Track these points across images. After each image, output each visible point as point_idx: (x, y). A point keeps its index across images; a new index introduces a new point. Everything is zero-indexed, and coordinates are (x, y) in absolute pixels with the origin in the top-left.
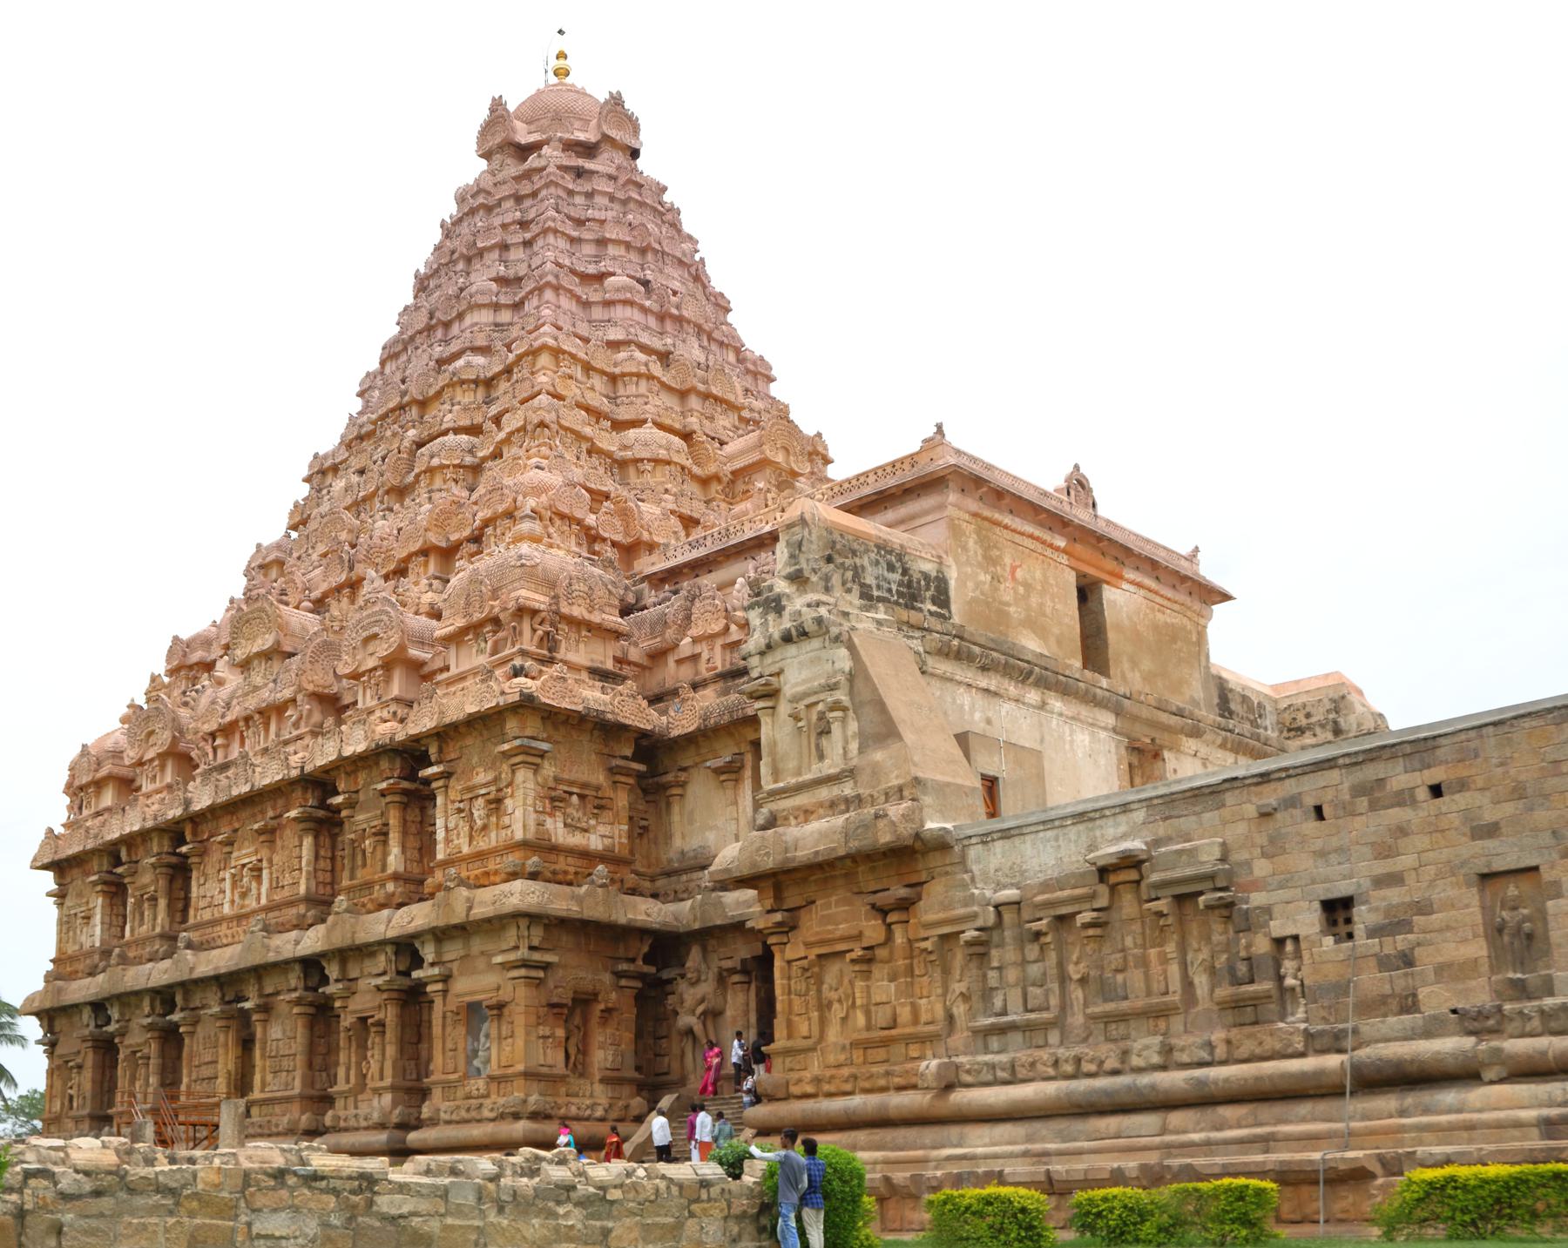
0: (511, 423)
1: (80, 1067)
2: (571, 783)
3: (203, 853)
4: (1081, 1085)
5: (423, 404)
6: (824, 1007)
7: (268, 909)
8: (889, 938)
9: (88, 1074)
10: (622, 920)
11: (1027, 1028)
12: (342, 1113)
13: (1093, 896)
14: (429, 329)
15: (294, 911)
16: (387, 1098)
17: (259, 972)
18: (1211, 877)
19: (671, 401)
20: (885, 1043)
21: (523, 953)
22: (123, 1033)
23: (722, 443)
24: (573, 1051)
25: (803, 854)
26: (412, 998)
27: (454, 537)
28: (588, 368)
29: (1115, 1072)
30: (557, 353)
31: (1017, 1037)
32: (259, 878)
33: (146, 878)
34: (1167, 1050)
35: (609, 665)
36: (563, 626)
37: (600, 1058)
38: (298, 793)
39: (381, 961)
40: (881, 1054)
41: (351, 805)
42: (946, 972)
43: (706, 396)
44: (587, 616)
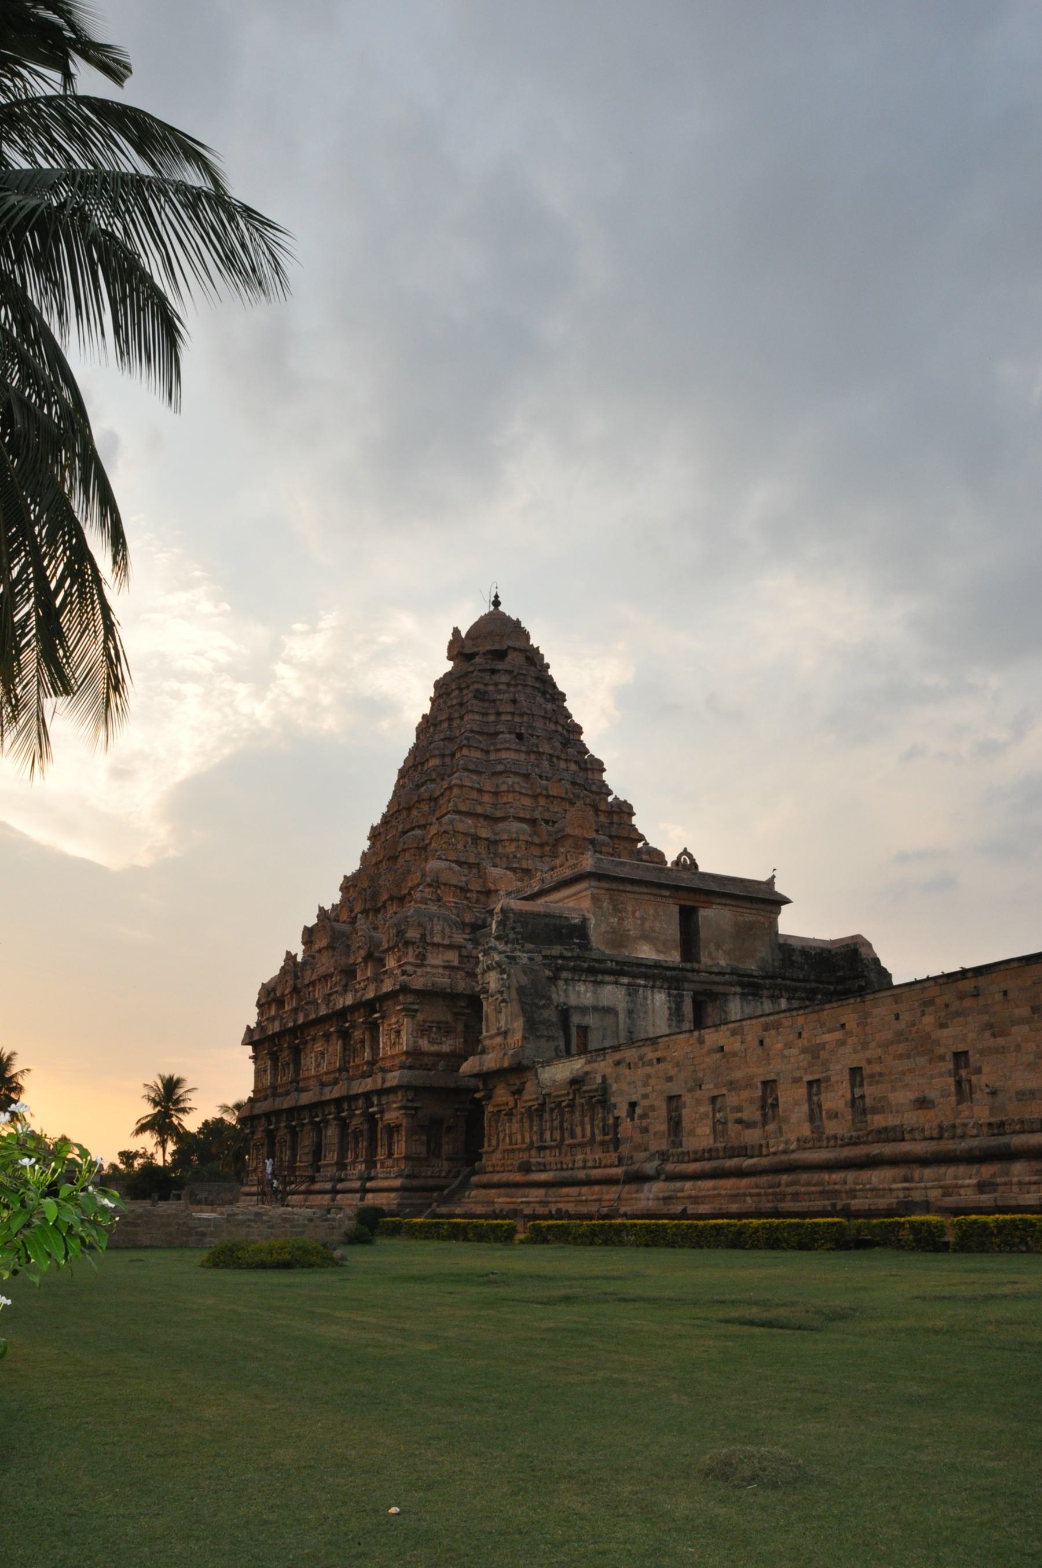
0: (433, 830)
1: (263, 1145)
2: (432, 1022)
3: (306, 1043)
4: (565, 1174)
5: (409, 809)
6: (498, 1134)
7: (326, 1074)
8: (516, 1106)
9: (265, 1149)
10: (453, 1085)
11: (550, 1148)
12: (349, 1172)
13: (568, 1094)
14: (415, 767)
15: (332, 1076)
16: (363, 1166)
17: (323, 1104)
18: (597, 1090)
19: (527, 802)
20: (513, 1151)
21: (404, 1103)
22: (277, 1129)
23: (554, 822)
24: (432, 1146)
25: (485, 1069)
26: (371, 1119)
27: (403, 892)
28: (480, 791)
29: (572, 1169)
30: (461, 786)
31: (548, 1152)
32: (323, 1058)
33: (286, 1053)
34: (585, 1161)
35: (456, 963)
36: (429, 948)
37: (446, 1149)
38: (334, 1020)
39: (360, 1103)
40: (511, 1155)
41: (353, 1027)
42: (531, 1121)
43: (548, 797)
44: (441, 942)
